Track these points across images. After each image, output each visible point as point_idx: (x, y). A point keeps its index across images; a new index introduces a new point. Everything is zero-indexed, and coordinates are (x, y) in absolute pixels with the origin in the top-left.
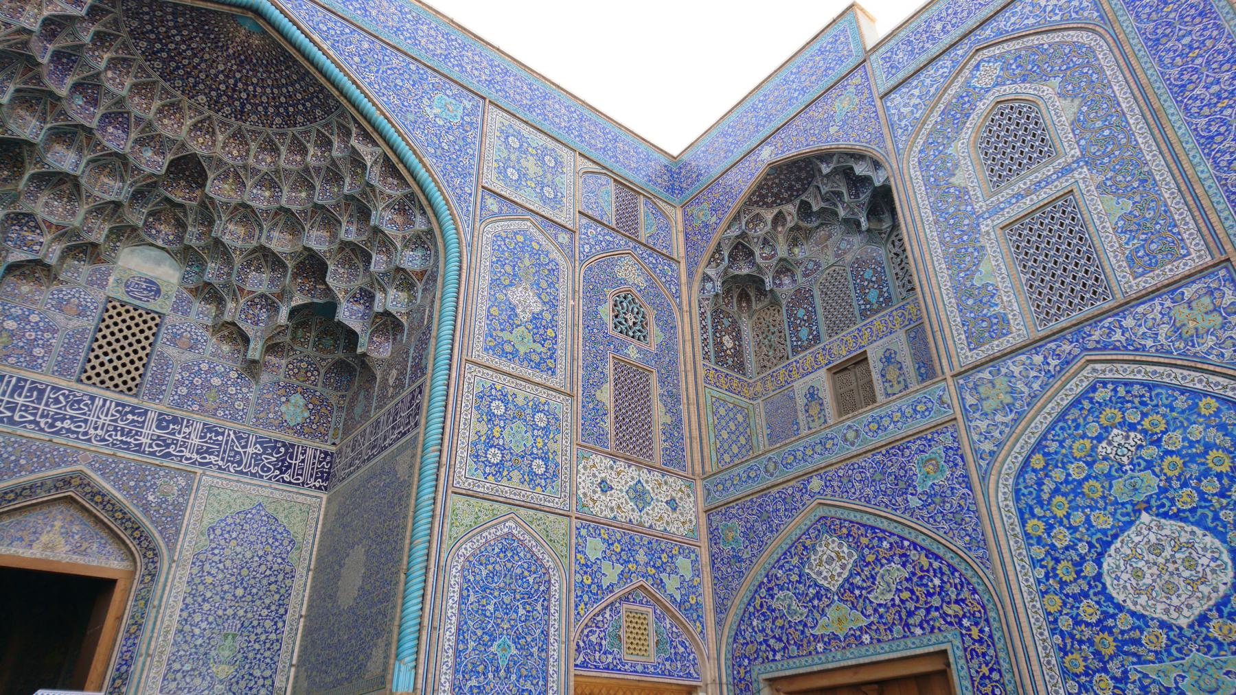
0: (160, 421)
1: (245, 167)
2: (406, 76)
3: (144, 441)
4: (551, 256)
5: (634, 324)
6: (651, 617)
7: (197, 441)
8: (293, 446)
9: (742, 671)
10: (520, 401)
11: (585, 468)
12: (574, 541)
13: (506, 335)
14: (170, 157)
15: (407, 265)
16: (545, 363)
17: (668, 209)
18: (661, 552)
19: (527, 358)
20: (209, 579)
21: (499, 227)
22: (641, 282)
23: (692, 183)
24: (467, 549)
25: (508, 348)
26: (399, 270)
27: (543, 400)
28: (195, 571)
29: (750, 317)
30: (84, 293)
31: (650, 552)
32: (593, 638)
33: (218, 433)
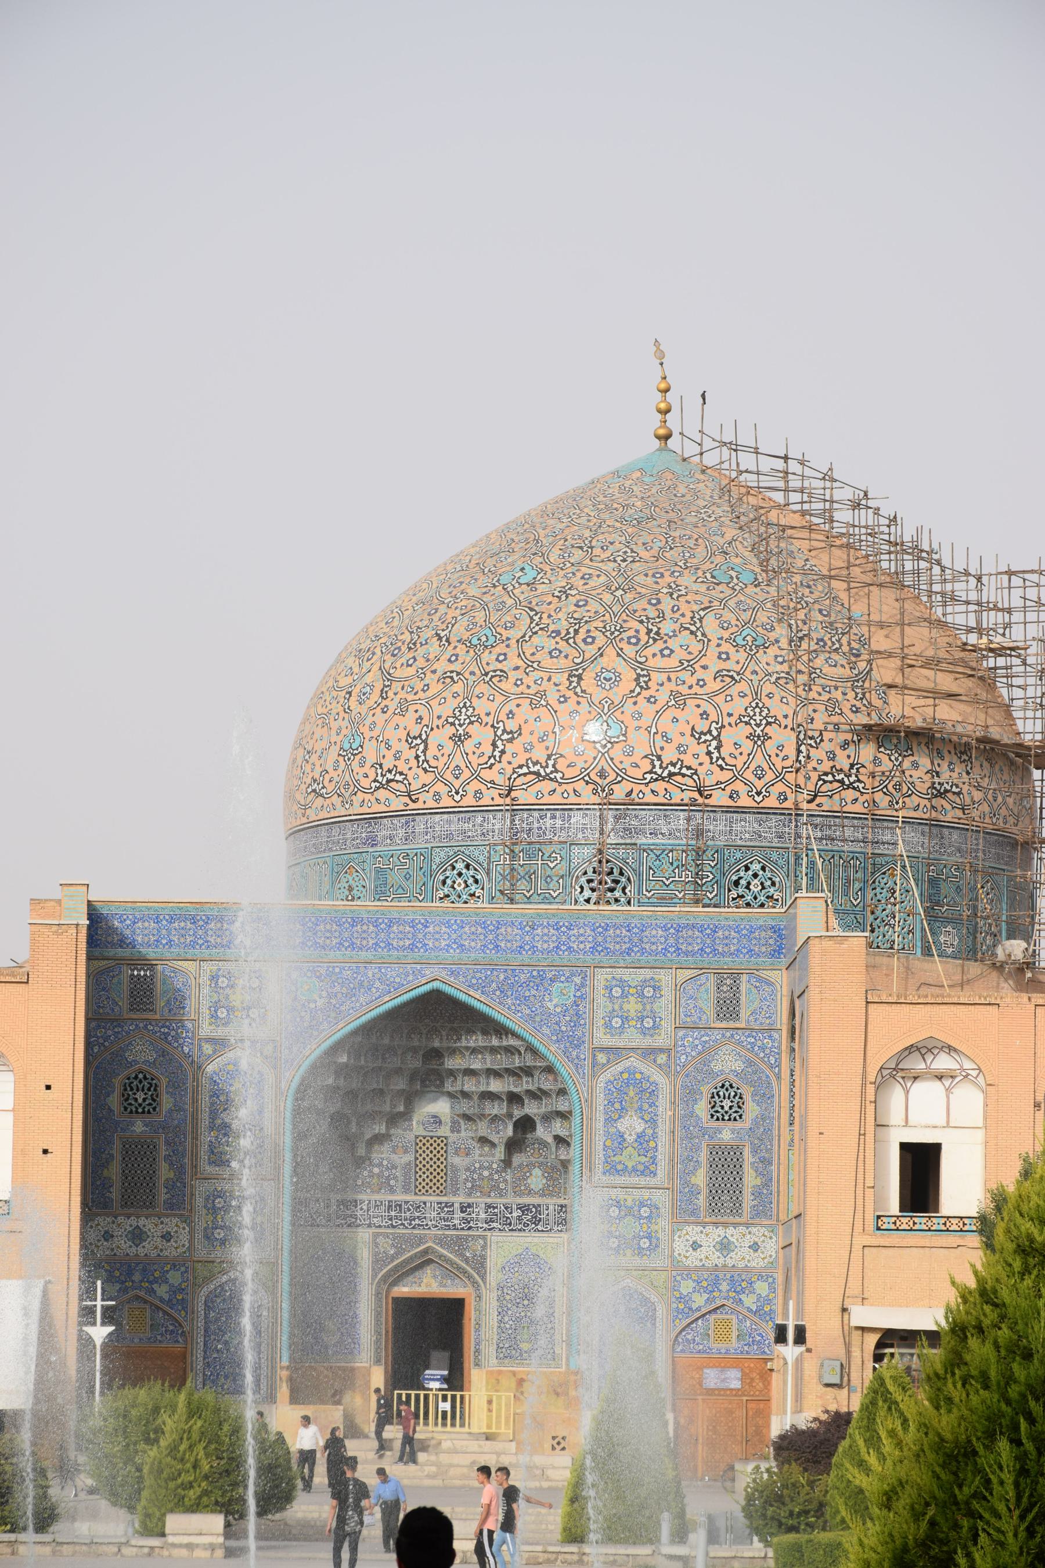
0: (461, 1208)
2: (532, 984)
3: (456, 1222)
4: (651, 1080)
5: (731, 1108)
6: (735, 1321)
7: (483, 1216)
8: (539, 1206)
10: (629, 1203)
11: (680, 1237)
13: (617, 1159)
14: (421, 1053)
16: (648, 1171)
18: (740, 1281)
19: (635, 1169)
20: (508, 1297)
22: (738, 1065)
25: (619, 1167)
27: (646, 1198)
28: (500, 1293)
32: (689, 1337)
33: (494, 1208)
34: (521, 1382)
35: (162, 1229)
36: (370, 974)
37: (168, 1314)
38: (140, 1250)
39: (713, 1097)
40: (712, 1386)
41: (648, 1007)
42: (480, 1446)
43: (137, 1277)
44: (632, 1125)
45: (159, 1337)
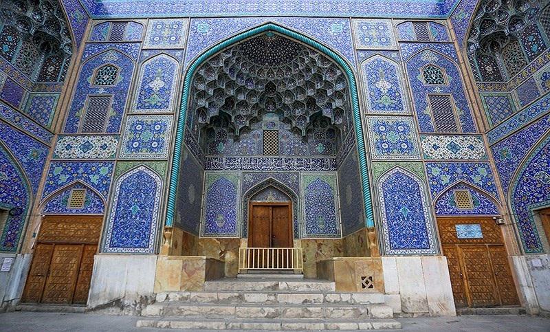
1: (284, 79)
5: (436, 78)
9: (521, 209)
10: (390, 124)
11: (425, 142)
12: (426, 170)
13: (379, 101)
15: (338, 89)
17: (442, 22)
18: (469, 167)
19: (390, 106)
21: (366, 62)
22: (436, 59)
23: (452, 5)
24: (383, 179)
26: (336, 92)
29: (500, 53)
30: (258, 130)
31: (463, 168)
34: (320, 245)
35: (102, 142)
36: (236, 21)
37: (97, 195)
38: (86, 154)
39: (425, 73)
40: (463, 236)
41: (382, 34)
42: (308, 286)
43: (80, 171)
44: (384, 85)
45: (89, 209)
